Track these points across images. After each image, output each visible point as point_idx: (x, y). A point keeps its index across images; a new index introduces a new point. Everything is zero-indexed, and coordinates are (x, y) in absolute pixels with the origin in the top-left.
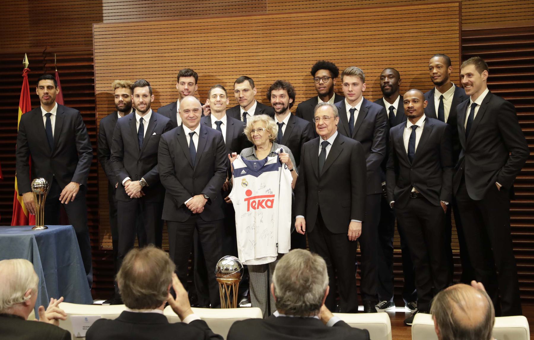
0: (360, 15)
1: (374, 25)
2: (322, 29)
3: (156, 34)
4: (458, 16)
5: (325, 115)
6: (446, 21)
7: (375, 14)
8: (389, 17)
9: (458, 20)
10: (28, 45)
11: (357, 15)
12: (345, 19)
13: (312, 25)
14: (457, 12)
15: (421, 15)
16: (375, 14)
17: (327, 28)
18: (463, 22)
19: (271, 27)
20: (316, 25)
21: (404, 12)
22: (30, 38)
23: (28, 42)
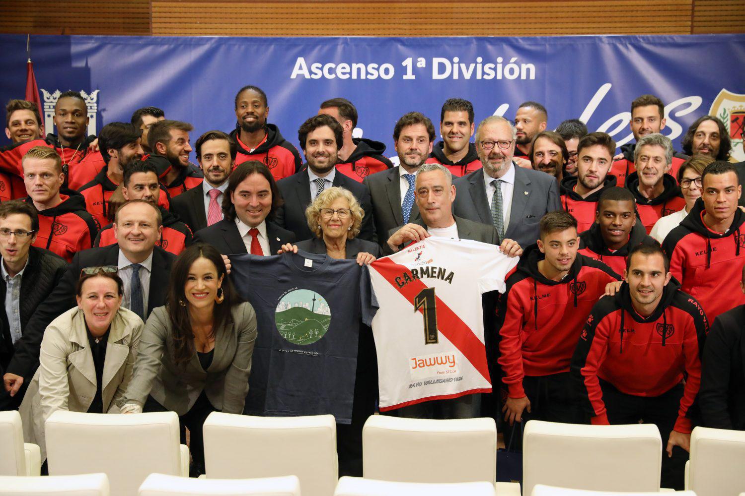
0: (554, 9)
1: (572, 25)
2: (497, 26)
3: (249, 21)
4: (690, 18)
5: (657, 155)
6: (674, 24)
7: (574, 9)
8: (594, 14)
9: (690, 23)
10: (31, 24)
11: (549, 9)
12: (532, 15)
13: (483, 21)
14: (690, 13)
15: (639, 14)
16: (574, 9)
17: (505, 26)
18: (695, 24)
19: (422, 20)
20: (489, 21)
21: (616, 9)
22: (34, 14)
23: (31, 19)
